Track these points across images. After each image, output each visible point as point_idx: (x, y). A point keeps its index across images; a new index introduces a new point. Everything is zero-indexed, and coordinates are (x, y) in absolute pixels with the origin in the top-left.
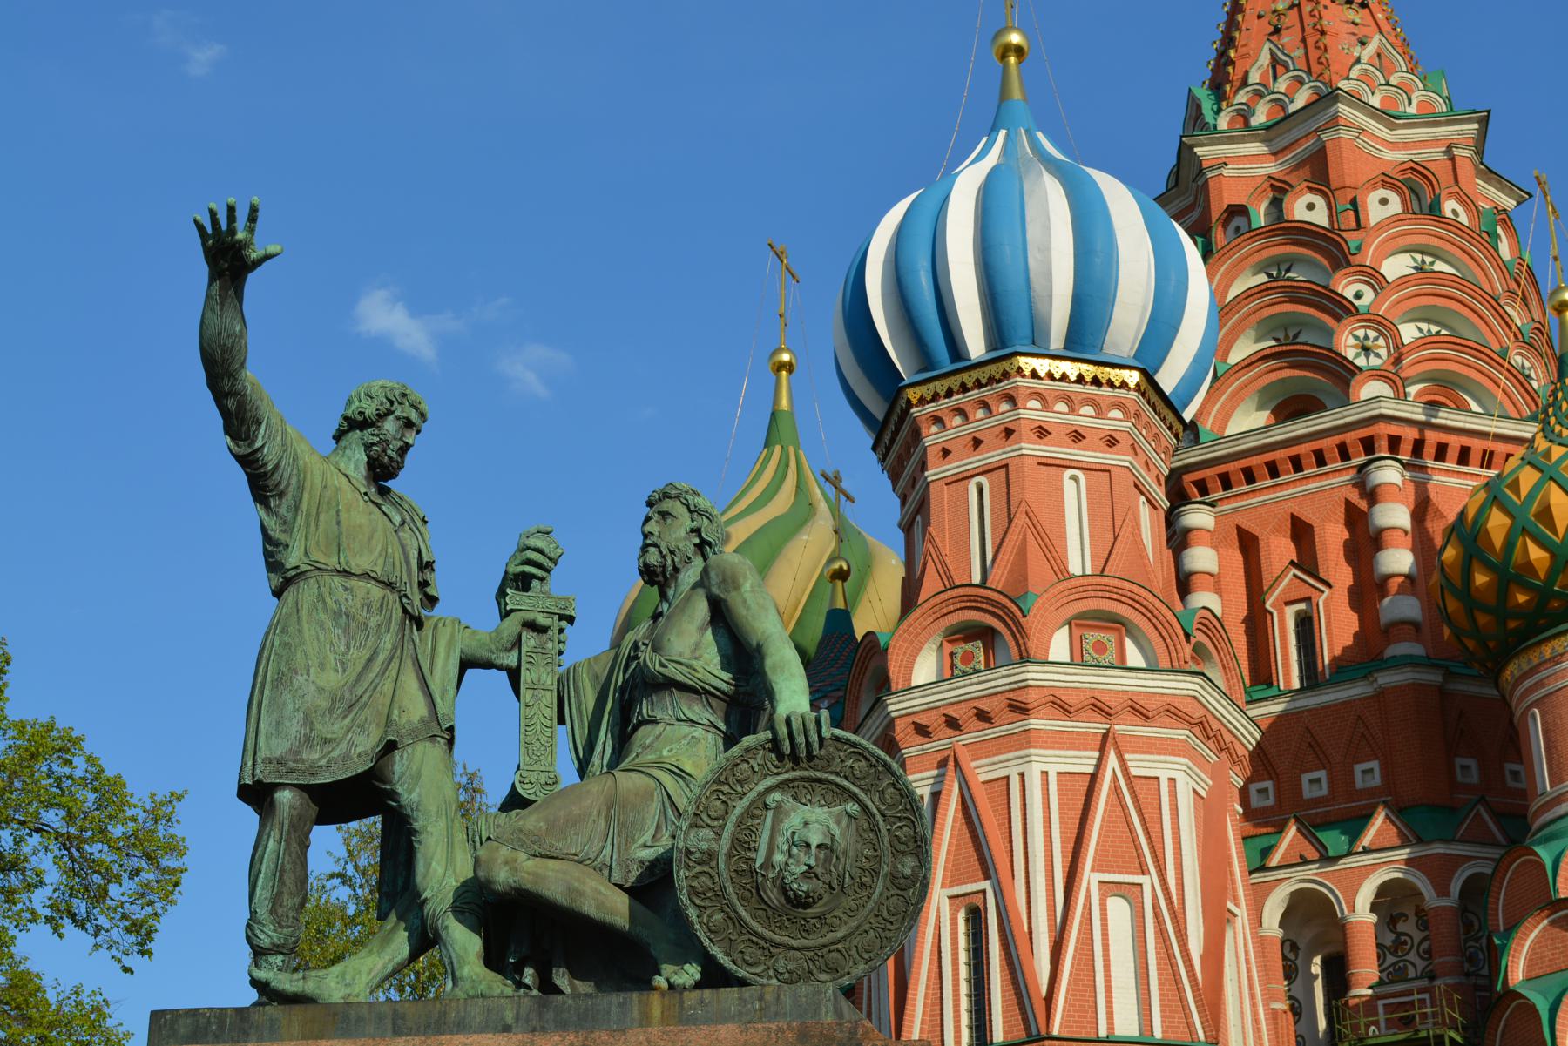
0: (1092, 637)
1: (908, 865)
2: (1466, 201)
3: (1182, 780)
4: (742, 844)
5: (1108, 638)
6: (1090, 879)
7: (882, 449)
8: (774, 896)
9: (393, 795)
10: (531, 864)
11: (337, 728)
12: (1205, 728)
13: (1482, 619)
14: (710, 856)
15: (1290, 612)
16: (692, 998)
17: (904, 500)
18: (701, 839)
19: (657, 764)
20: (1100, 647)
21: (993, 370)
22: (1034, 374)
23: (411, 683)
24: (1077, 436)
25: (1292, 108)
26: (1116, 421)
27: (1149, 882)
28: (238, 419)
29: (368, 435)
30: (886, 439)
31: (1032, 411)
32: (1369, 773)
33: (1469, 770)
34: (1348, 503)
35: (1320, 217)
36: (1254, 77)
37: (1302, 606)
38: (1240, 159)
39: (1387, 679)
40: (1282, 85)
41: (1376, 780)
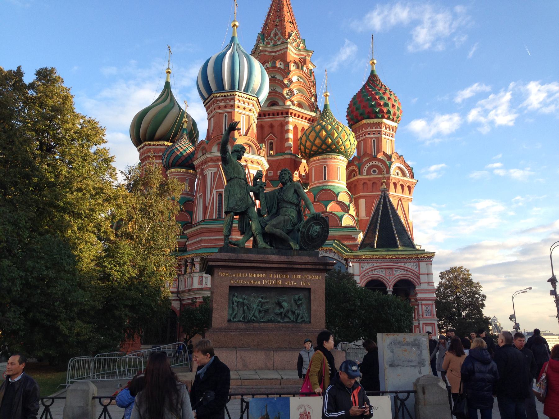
2: (307, 68)
4: (308, 231)
7: (205, 103)
8: (310, 238)
9: (248, 215)
11: (239, 203)
13: (307, 151)
15: (269, 141)
16: (300, 251)
17: (209, 114)
19: (289, 214)
21: (231, 93)
22: (239, 96)
25: (279, 43)
26: (251, 107)
29: (238, 153)
30: (207, 102)
34: (281, 123)
35: (282, 67)
36: (272, 35)
37: (272, 141)
38: (268, 51)
40: (277, 37)
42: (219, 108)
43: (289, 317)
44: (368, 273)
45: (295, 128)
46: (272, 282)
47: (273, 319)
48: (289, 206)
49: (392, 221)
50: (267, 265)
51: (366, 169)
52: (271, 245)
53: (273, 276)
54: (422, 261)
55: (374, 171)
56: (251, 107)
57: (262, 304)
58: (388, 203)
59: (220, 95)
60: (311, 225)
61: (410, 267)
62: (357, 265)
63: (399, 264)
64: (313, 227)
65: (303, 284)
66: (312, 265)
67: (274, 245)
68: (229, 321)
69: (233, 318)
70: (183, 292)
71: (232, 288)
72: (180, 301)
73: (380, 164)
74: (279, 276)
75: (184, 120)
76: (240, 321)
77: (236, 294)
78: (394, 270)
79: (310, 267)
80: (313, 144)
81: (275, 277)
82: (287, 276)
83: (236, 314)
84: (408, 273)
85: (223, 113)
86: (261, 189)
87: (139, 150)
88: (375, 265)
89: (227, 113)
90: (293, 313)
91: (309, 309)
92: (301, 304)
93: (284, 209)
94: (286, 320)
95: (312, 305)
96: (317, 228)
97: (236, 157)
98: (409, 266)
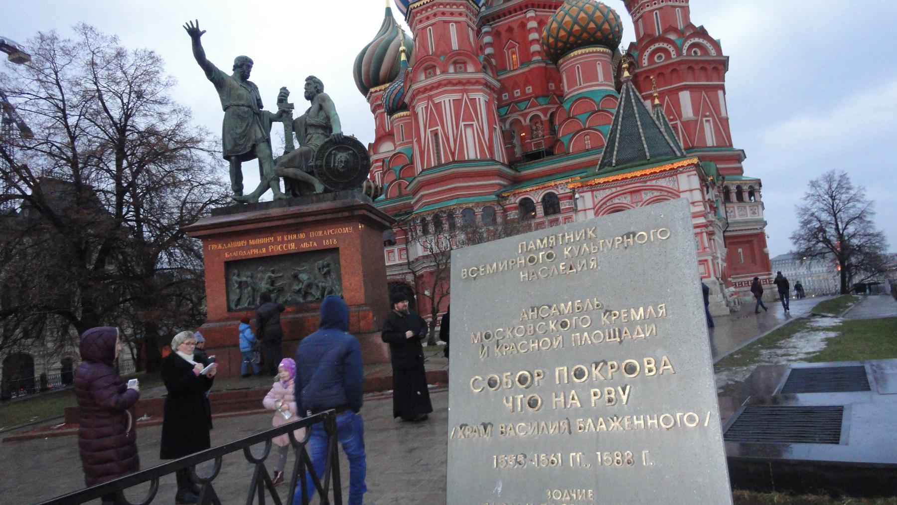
0: (458, 66)
1: (365, 162)
3: (481, 98)
4: (328, 162)
5: (462, 65)
6: (462, 124)
10: (286, 170)
11: (242, 142)
12: (487, 85)
14: (321, 166)
18: (319, 163)
20: (461, 68)
23: (258, 129)
24: (452, 14)
27: (475, 123)
28: (210, 70)
29: (239, 70)
31: (441, 8)
32: (529, 89)
33: (552, 86)
39: (532, 66)
41: (531, 91)
42: (421, 21)
43: (311, 294)
44: (604, 203)
45: (541, 23)
46: (282, 248)
47: (290, 299)
48: (310, 131)
49: (639, 123)
50: (267, 224)
51: (646, 58)
52: (295, 195)
53: (283, 238)
54: (681, 172)
55: (660, 57)
56: (462, 9)
57: (272, 282)
58: (632, 97)
59: (418, 4)
60: (330, 154)
61: (664, 185)
62: (588, 196)
63: (649, 183)
64: (335, 155)
65: (327, 243)
66: (332, 213)
67: (298, 193)
68: (229, 310)
69: (236, 306)
70: (413, 262)
71: (230, 265)
72: (414, 273)
73: (665, 46)
74: (290, 237)
75: (402, 48)
76: (246, 309)
77: (236, 271)
78: (643, 192)
79: (329, 216)
80: (557, 39)
81: (285, 239)
82: (302, 236)
83: (239, 300)
84: (664, 193)
85: (425, 28)
86: (284, 115)
87: (368, 99)
88: (614, 190)
89: (432, 25)
90: (318, 286)
91: (339, 279)
92: (329, 272)
93: (309, 137)
94: (310, 299)
95: (343, 272)
96: (342, 156)
97: (238, 75)
98: (663, 182)
